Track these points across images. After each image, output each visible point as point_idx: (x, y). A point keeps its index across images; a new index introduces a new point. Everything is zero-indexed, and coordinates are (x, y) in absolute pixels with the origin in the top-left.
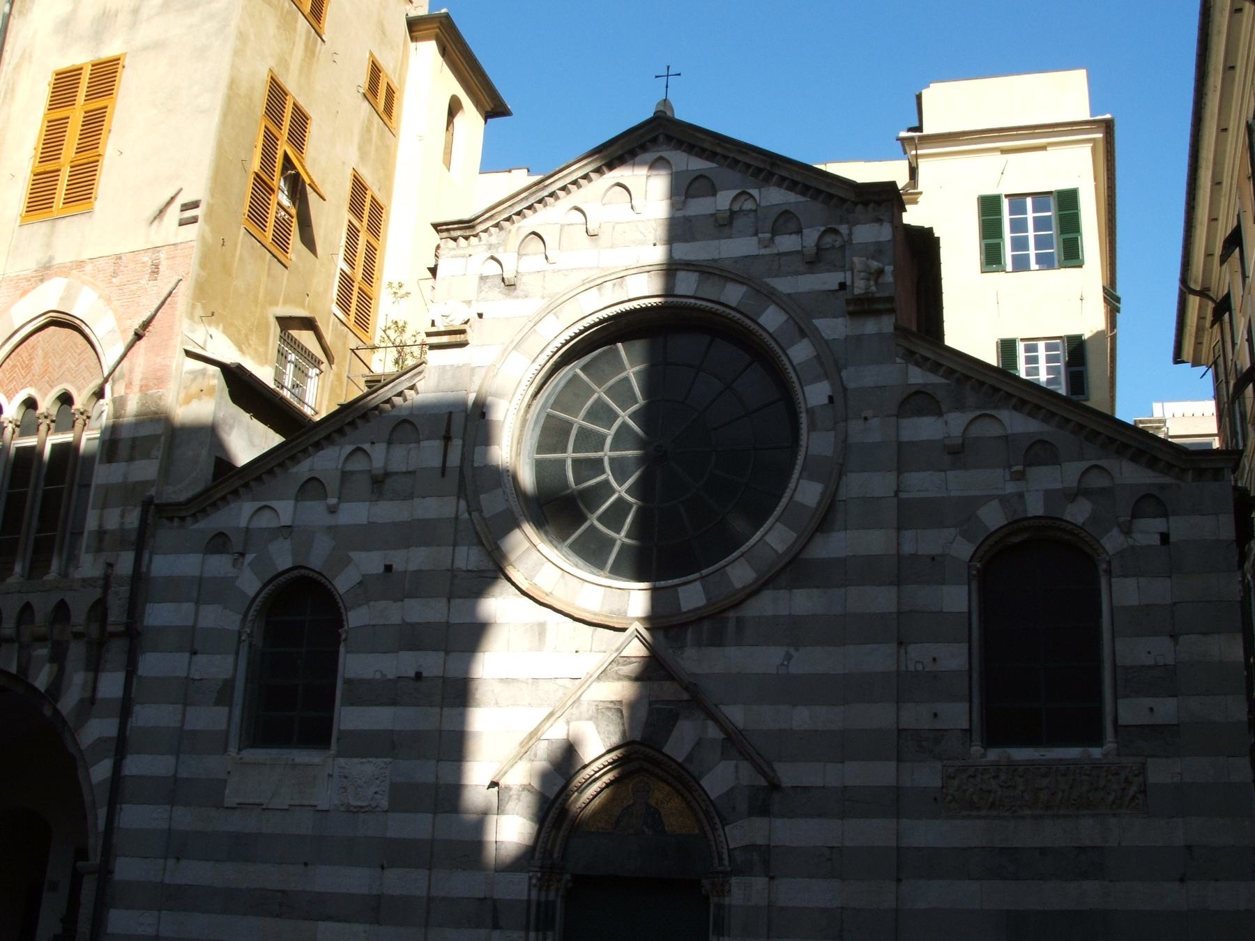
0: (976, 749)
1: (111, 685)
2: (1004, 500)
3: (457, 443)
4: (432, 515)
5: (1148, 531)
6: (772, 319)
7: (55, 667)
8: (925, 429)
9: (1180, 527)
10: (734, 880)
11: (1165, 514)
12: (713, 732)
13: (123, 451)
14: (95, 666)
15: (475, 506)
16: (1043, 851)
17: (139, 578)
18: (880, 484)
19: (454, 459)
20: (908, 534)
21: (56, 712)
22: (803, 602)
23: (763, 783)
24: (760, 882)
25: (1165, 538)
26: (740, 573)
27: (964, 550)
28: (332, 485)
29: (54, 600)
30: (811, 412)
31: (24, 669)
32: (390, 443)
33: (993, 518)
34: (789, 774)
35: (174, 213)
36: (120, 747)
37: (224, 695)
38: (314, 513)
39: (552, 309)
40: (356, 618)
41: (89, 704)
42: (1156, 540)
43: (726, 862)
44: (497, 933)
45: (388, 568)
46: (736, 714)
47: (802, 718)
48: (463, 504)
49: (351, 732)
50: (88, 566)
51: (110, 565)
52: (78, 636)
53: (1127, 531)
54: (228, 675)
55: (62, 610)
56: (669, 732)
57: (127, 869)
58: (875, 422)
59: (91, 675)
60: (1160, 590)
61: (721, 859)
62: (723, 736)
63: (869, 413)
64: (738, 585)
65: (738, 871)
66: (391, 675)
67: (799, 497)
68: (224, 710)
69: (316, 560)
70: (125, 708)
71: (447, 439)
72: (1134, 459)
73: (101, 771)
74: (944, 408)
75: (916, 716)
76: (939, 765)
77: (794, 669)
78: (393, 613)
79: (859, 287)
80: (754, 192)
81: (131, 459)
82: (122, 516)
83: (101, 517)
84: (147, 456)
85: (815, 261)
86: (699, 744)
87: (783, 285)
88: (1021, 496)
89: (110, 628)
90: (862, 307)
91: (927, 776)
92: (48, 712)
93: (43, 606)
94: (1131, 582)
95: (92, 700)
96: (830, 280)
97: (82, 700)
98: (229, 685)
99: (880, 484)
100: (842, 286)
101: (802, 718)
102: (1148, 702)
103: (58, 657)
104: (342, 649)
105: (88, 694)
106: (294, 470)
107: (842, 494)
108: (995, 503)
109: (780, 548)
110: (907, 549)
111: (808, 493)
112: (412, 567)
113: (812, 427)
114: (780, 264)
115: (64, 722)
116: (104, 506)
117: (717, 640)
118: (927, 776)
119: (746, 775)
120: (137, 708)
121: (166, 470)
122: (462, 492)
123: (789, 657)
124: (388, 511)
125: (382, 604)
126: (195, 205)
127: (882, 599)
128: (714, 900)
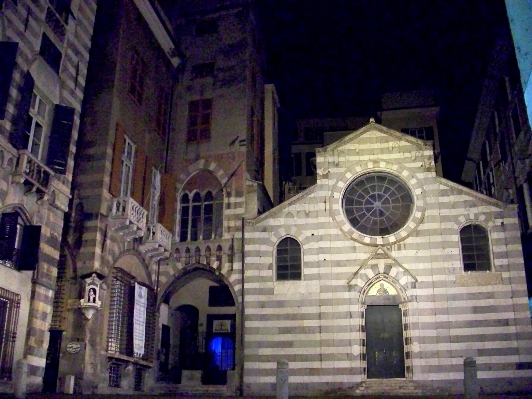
0: (463, 271)
1: (237, 266)
2: (465, 215)
3: (328, 204)
4: (324, 221)
5: (499, 222)
6: (405, 174)
7: (218, 262)
8: (445, 199)
9: (506, 221)
10: (409, 303)
11: (503, 218)
12: (401, 270)
13: (232, 206)
14: (231, 261)
15: (334, 219)
16: (480, 293)
17: (243, 239)
18: (435, 212)
19: (328, 207)
20: (443, 224)
21: (220, 273)
22: (418, 240)
23: (414, 281)
24: (415, 304)
25: (502, 223)
26: (403, 232)
27: (457, 228)
28: (295, 214)
29: (216, 245)
30: (417, 196)
31: (208, 264)
32: (309, 204)
33: (462, 219)
34: (419, 279)
35: (237, 142)
36: (242, 281)
37: (270, 267)
38: (291, 221)
39: (349, 170)
40: (305, 247)
41: (231, 270)
42: (501, 224)
43: (406, 299)
44: (351, 319)
45: (313, 235)
46: (406, 266)
47: (421, 266)
48: (331, 219)
49: (307, 275)
50: (226, 236)
51: (234, 236)
52: (225, 254)
53: (494, 222)
54: (271, 262)
55: (220, 248)
56: (390, 271)
57: (248, 311)
58: (433, 198)
59: (230, 264)
60: (502, 235)
61: (405, 299)
62: (403, 271)
63: (431, 196)
64: (403, 236)
65: (410, 301)
66: (317, 260)
67: (416, 216)
68: (271, 271)
69: (293, 233)
70: (243, 271)
71: (325, 202)
72: (494, 205)
73: (237, 288)
74: (449, 194)
75: (447, 265)
76: (455, 276)
77: (419, 255)
78: (315, 245)
79: (427, 166)
80: (398, 142)
81: (235, 208)
82: (235, 222)
83: (228, 223)
84: (240, 207)
85: (415, 160)
86: (398, 273)
87: (407, 165)
88: (469, 215)
89: (235, 252)
90: (428, 170)
91: (452, 278)
92: (217, 273)
93: (213, 247)
94: (495, 233)
95: (232, 270)
96: (418, 164)
97: (228, 271)
98: (271, 264)
99: (435, 212)
100: (422, 165)
101: (421, 266)
102: (501, 260)
103: (219, 259)
104: (302, 255)
105: (230, 269)
106: (284, 210)
107: (426, 215)
108: (463, 216)
109: (413, 227)
110: (443, 227)
111: (418, 215)
112: (320, 234)
113: (418, 199)
114: (405, 160)
115: (223, 275)
116: (229, 220)
117: (399, 249)
118: (452, 278)
119: (410, 279)
120: (245, 271)
121: (246, 212)
122: (330, 216)
123: (417, 252)
124: (311, 221)
125: (312, 243)
126: (244, 141)
127: (438, 239)
128: (403, 309)
